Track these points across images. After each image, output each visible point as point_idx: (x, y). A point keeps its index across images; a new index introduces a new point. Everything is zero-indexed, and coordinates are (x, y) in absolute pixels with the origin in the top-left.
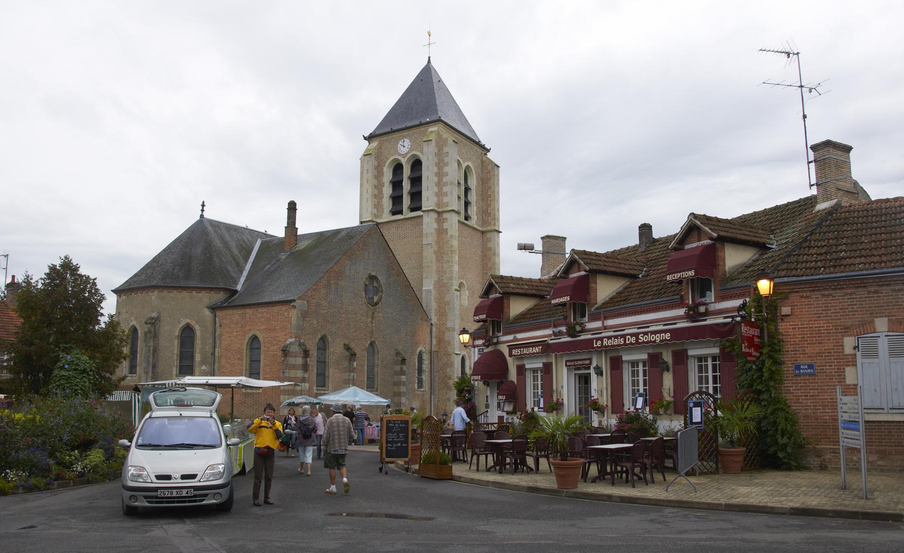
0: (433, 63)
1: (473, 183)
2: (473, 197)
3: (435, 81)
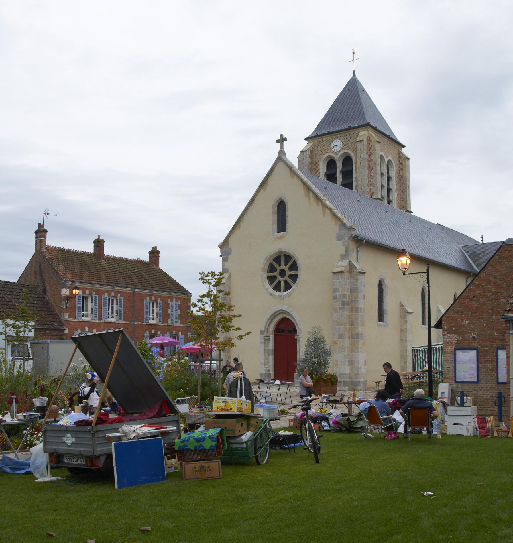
0: (358, 76)
1: (393, 173)
2: (394, 185)
3: (360, 90)
